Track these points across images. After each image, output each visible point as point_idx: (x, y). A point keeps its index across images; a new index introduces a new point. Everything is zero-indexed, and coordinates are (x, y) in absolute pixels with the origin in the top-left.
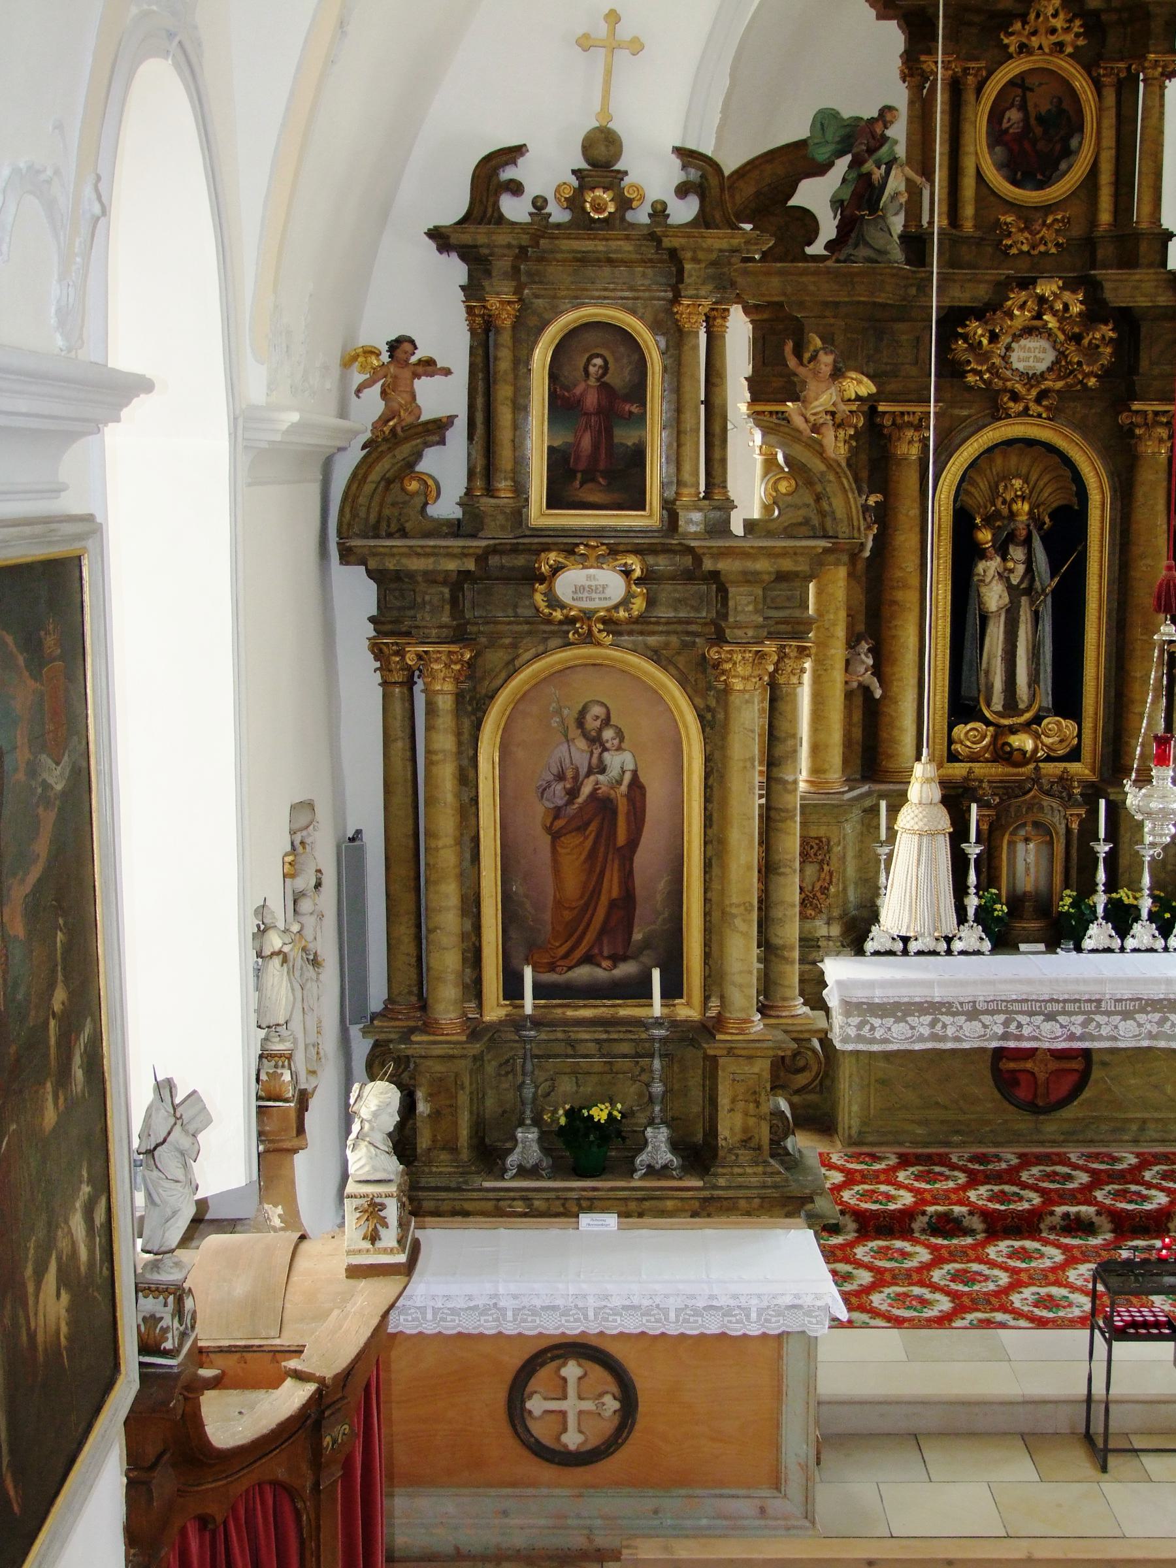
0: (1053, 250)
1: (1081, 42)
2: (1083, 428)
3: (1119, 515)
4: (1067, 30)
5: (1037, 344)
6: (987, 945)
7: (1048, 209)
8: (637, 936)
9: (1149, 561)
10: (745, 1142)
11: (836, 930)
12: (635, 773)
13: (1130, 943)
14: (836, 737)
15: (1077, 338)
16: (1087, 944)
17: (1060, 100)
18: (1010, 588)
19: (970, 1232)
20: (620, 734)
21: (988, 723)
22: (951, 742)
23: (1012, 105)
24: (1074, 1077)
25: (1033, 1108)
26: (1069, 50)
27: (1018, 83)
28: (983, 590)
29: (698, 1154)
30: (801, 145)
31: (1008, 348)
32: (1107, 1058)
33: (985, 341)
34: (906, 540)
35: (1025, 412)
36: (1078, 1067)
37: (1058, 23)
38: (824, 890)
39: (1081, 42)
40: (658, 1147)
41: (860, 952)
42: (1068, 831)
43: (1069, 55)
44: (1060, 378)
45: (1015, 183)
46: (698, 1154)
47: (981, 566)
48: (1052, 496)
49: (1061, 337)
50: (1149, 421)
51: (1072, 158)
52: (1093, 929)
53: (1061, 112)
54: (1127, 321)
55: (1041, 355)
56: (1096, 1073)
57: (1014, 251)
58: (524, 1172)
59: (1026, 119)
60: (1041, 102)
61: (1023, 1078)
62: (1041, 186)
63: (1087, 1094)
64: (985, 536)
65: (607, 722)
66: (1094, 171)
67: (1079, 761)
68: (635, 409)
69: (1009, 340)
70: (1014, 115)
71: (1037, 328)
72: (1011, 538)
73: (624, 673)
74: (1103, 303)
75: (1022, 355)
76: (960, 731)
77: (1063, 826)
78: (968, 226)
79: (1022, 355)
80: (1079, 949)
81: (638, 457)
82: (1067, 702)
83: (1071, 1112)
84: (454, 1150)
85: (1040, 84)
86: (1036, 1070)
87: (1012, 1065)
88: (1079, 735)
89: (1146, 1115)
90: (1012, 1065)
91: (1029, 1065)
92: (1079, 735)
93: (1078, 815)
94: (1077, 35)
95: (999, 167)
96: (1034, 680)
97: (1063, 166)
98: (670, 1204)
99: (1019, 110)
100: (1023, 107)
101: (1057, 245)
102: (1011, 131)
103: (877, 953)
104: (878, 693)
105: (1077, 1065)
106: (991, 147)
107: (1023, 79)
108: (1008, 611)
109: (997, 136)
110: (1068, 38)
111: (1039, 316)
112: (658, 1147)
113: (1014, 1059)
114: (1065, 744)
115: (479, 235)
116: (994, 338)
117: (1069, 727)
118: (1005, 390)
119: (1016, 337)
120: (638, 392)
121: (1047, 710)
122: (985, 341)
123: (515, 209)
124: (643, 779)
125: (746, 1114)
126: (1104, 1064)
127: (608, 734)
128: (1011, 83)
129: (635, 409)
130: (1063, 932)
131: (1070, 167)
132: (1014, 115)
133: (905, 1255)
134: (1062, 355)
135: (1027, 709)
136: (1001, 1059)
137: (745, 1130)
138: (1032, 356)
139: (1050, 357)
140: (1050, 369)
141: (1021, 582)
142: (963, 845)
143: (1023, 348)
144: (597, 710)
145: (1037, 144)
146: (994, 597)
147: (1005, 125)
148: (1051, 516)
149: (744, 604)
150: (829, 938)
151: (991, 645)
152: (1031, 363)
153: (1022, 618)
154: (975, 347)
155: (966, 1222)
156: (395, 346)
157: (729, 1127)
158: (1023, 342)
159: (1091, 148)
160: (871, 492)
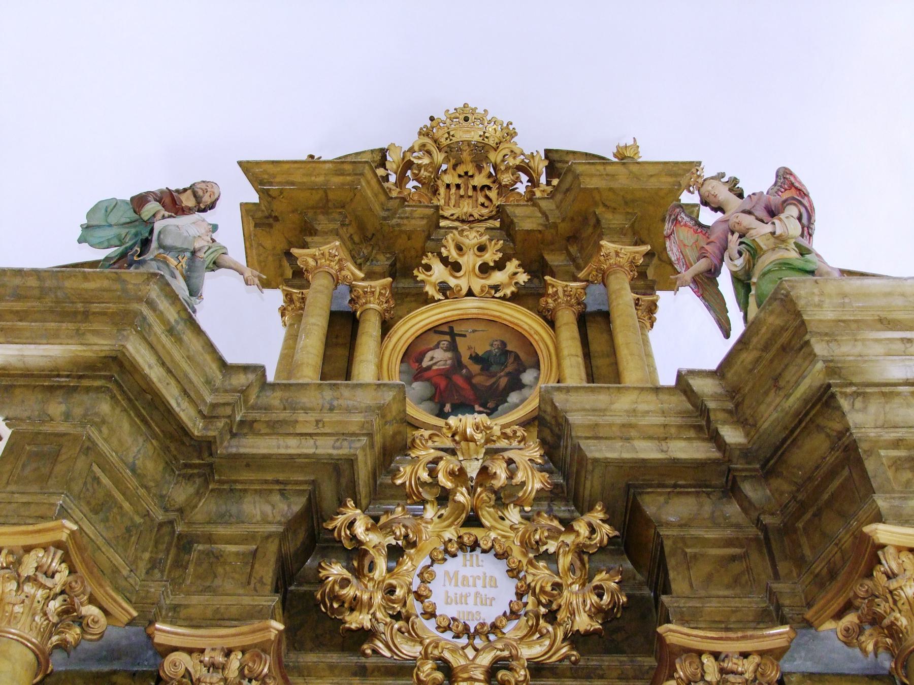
5: (478, 571)
17: (504, 344)
23: (437, 346)
31: (425, 576)
51: (525, 391)
54: (629, 498)
55: (489, 592)
60: (478, 343)
75: (452, 590)
79: (452, 590)
85: (474, 331)
100: (453, 347)
102: (435, 367)
107: (451, 328)
128: (435, 330)
131: (522, 401)
139: (504, 593)
143: (452, 578)
147: (426, 363)
152: (471, 607)
158: (452, 565)
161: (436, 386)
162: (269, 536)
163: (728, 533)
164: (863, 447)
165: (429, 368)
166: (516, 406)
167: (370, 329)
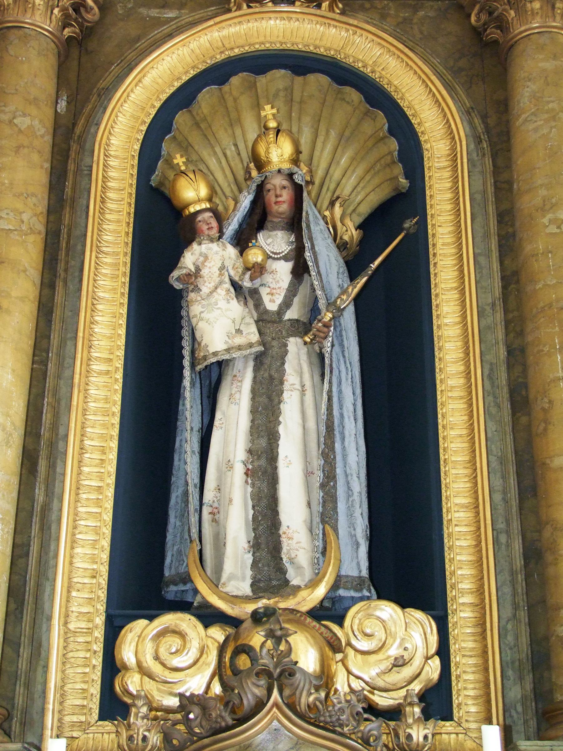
3: (490, 181)
18: (264, 320)
21: (209, 616)
22: (112, 668)
28: (195, 309)
47: (189, 259)
72: (258, 218)
76: (138, 640)
82: (405, 566)
88: (443, 651)
92: (443, 651)
108: (259, 359)
114: (407, 672)
121: (358, 584)
135: (313, 584)
141: (287, 304)
146: (218, 323)
151: (225, 443)
153: (291, 378)
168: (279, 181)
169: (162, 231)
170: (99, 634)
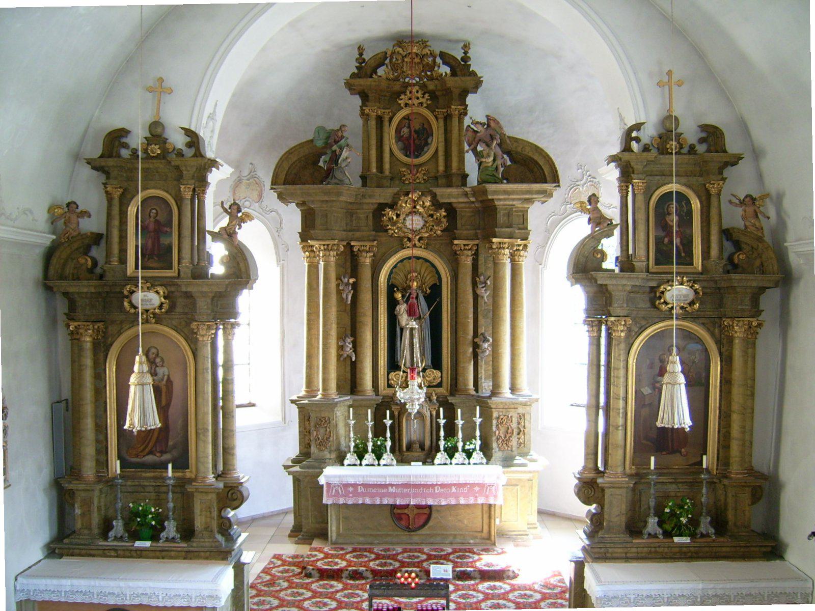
0: (422, 182)
1: (429, 102)
2: (438, 252)
4: (423, 97)
6: (395, 462)
7: (420, 165)
8: (171, 443)
9: (464, 305)
10: (207, 528)
11: (333, 456)
12: (168, 376)
13: (454, 461)
14: (333, 375)
15: (432, 216)
16: (436, 461)
19: (363, 578)
20: (162, 360)
22: (388, 380)
24: (425, 517)
25: (408, 529)
26: (425, 105)
27: (406, 118)
28: (399, 317)
29: (187, 532)
30: (312, 141)
31: (404, 219)
32: (439, 509)
33: (395, 218)
34: (366, 297)
35: (415, 246)
36: (427, 512)
37: (419, 95)
38: (328, 439)
39: (429, 102)
40: (171, 529)
41: (342, 465)
42: (431, 415)
43: (425, 107)
44: (426, 232)
45: (407, 156)
46: (187, 532)
47: (398, 308)
48: (430, 280)
49: (425, 215)
50: (462, 248)
51: (429, 146)
52: (439, 455)
53: (424, 129)
56: (434, 515)
57: (407, 182)
58: (116, 539)
59: (410, 132)
60: (416, 125)
61: (403, 516)
62: (417, 157)
63: (431, 523)
64: (399, 296)
65: (157, 355)
66: (437, 151)
67: (442, 387)
68: (168, 230)
69: (404, 216)
70: (405, 130)
71: (415, 212)
73: (164, 336)
74: (438, 201)
76: (392, 375)
77: (429, 413)
78: (387, 173)
80: (433, 464)
81: (169, 249)
82: (436, 363)
83: (424, 531)
84: (90, 529)
85: (415, 118)
86: (409, 513)
87: (399, 511)
88: (441, 377)
89: (455, 533)
90: (399, 511)
91: (406, 511)
93: (435, 408)
94: (427, 100)
95: (401, 150)
96: (423, 354)
97: (426, 149)
98: (173, 554)
99: (408, 128)
100: (409, 127)
101: (424, 179)
103: (349, 465)
104: (354, 359)
105: (427, 511)
106: (397, 142)
109: (399, 138)
110: (423, 100)
111: (415, 207)
112: (171, 529)
113: (400, 509)
115: (111, 162)
116: (398, 216)
117: (437, 373)
118: (405, 237)
119: (407, 215)
120: (169, 223)
121: (429, 366)
122: (395, 218)
123: (125, 153)
124: (172, 378)
125: (206, 517)
126: (438, 511)
127: (158, 360)
128: (404, 118)
129: (168, 230)
130: (428, 458)
132: (405, 130)
133: (332, 586)
134: (426, 222)
136: (394, 508)
137: (206, 523)
138: (415, 222)
139: (421, 223)
140: (422, 228)
142: (384, 421)
144: (153, 350)
145: (415, 141)
147: (402, 134)
148: (430, 288)
149: (203, 305)
150: (330, 459)
154: (391, 219)
155: (364, 574)
156: (68, 205)
157: (199, 522)
159: (436, 141)
160: (351, 277)
161: (405, 144)
162: (369, 212)
163: (471, 210)
164: (498, 210)
165: (403, 136)
166: (426, 152)
167: (386, 123)
168: (414, 291)
169: (392, 304)
170: (386, 375)
